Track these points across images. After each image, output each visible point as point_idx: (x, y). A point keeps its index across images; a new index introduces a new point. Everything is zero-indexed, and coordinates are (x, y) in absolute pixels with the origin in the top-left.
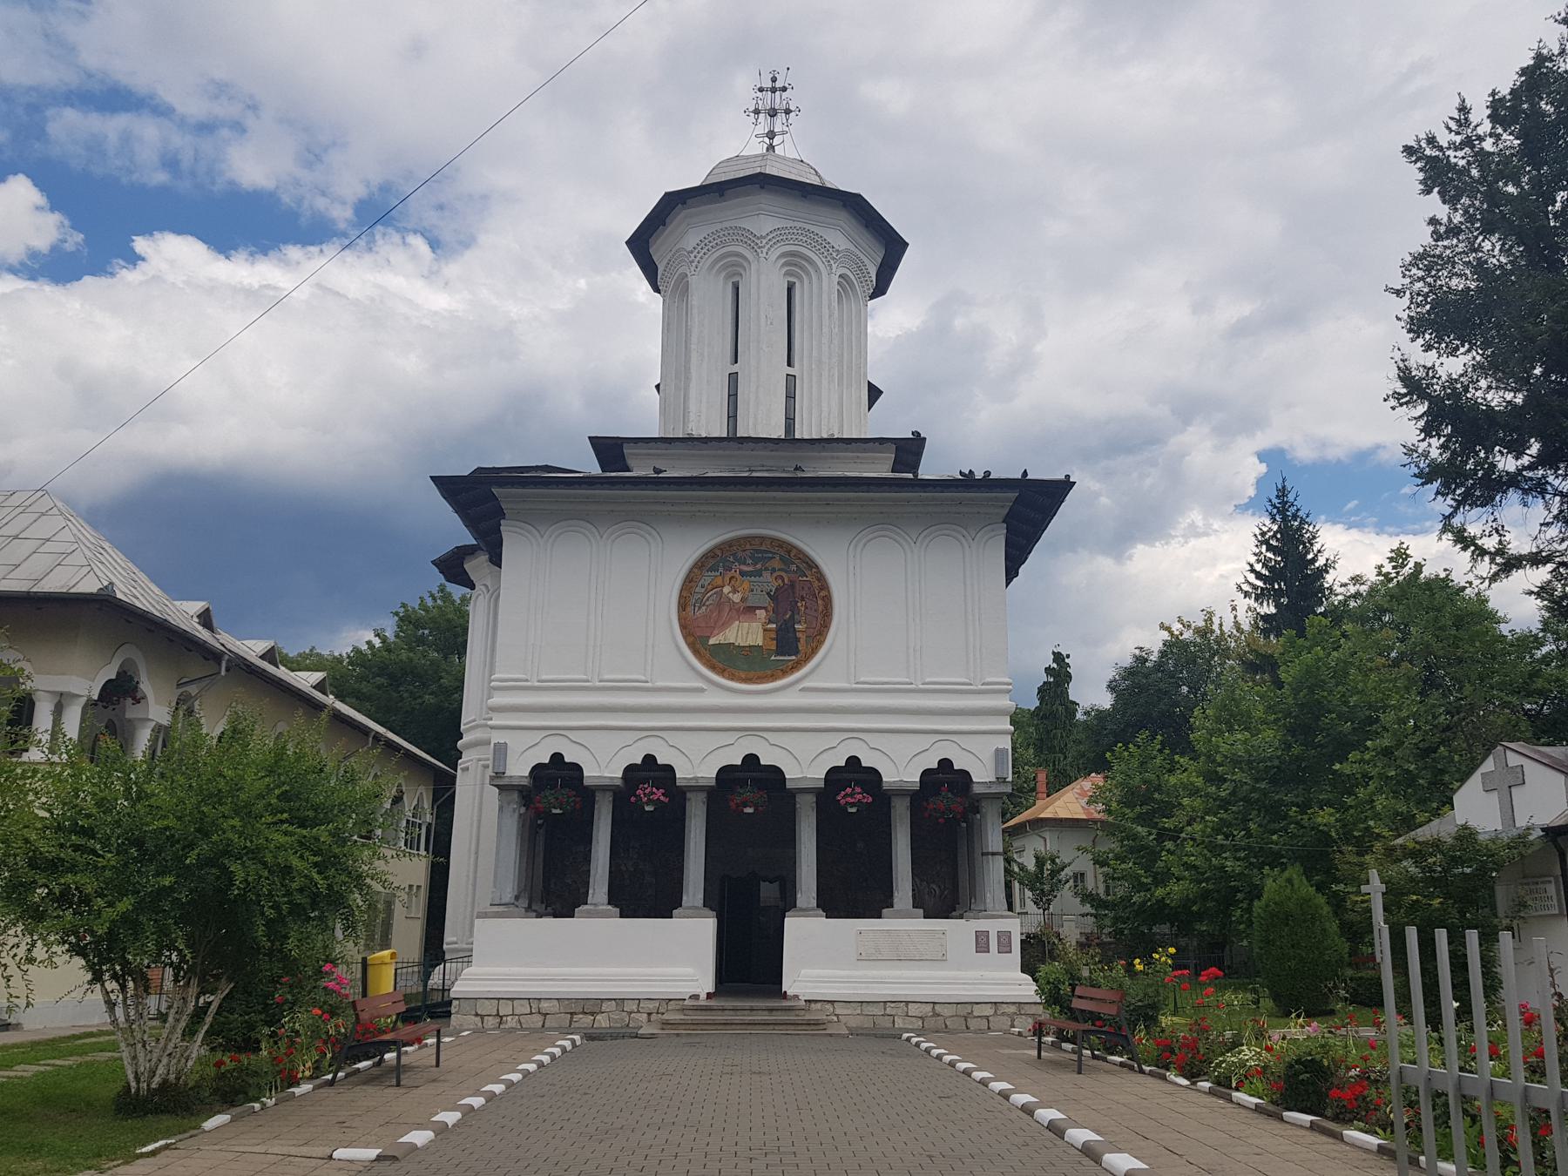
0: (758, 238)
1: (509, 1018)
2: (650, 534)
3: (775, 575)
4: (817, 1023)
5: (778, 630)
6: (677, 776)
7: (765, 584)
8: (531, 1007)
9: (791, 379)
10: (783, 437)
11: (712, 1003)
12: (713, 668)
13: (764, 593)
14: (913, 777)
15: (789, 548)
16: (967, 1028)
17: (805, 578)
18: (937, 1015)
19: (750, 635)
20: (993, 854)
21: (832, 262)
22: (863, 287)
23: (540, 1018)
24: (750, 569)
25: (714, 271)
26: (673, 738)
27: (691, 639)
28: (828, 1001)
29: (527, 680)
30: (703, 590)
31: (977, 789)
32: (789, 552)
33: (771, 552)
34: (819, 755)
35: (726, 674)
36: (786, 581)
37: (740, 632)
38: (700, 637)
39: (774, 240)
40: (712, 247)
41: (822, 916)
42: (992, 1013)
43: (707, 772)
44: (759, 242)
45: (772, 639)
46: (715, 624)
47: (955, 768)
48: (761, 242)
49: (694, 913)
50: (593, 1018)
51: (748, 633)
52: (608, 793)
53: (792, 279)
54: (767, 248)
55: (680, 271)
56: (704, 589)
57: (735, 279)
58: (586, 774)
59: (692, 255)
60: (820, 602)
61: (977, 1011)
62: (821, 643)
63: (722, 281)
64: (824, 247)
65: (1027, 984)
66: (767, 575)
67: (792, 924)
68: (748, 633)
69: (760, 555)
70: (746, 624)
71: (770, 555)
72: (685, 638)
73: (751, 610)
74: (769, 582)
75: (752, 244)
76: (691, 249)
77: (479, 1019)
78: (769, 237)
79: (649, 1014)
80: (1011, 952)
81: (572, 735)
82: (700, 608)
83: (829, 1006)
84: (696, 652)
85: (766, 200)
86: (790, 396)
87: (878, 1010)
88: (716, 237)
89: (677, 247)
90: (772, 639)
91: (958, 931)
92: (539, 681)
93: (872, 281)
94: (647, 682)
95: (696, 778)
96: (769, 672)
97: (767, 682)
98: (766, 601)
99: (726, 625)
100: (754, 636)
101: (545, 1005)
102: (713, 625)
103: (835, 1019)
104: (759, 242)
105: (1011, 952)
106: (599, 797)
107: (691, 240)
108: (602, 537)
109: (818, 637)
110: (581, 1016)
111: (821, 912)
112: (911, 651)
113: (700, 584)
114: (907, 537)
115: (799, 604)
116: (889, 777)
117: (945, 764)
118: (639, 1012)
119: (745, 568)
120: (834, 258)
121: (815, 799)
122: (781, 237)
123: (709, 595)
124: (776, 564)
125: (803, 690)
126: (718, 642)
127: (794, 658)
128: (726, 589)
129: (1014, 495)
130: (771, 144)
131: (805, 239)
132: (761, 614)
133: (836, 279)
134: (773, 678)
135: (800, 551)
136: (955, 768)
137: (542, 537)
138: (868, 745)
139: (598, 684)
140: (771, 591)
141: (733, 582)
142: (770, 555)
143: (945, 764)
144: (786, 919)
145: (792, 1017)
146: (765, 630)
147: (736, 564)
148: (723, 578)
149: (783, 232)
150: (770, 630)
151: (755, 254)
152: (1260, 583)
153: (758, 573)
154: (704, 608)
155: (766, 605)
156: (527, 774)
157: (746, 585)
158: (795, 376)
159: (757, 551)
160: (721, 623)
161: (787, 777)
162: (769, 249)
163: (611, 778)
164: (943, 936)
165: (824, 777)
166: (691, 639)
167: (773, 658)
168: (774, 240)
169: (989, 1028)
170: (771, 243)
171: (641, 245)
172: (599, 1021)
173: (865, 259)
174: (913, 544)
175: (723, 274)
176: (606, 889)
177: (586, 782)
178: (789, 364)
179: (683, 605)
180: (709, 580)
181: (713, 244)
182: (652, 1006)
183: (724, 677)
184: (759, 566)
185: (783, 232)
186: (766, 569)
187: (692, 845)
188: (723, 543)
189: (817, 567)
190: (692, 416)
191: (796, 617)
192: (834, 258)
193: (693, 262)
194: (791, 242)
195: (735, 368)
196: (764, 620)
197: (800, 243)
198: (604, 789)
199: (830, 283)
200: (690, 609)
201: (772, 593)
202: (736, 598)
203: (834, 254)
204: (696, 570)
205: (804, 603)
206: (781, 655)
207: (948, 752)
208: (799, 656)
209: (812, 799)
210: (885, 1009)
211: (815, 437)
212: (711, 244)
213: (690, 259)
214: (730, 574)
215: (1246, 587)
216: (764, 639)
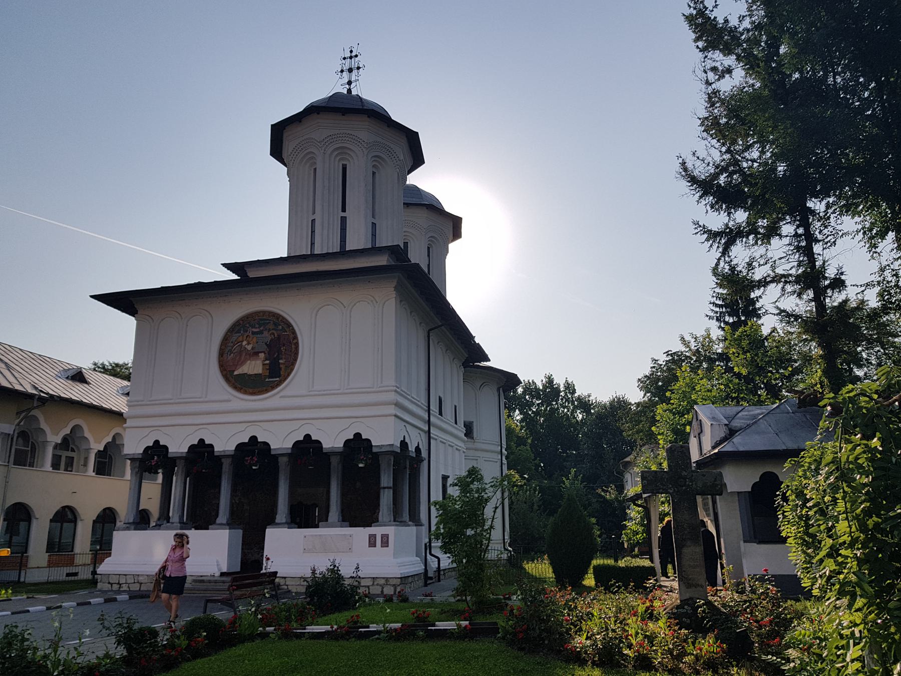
1: (124, 585)
3: (271, 332)
5: (270, 364)
6: (215, 450)
11: (224, 579)
14: (339, 444)
20: (384, 488)
21: (364, 149)
23: (138, 585)
25: (305, 161)
27: (225, 372)
28: (283, 577)
29: (142, 401)
31: (375, 450)
32: (278, 319)
33: (267, 320)
34: (289, 434)
35: (242, 390)
38: (230, 371)
39: (329, 142)
41: (285, 528)
42: (371, 583)
43: (231, 447)
44: (319, 144)
45: (267, 369)
47: (363, 438)
49: (221, 526)
52: (182, 461)
54: (323, 148)
58: (170, 451)
60: (293, 346)
62: (292, 370)
66: (266, 334)
67: (270, 532)
68: (254, 367)
70: (254, 362)
71: (268, 321)
72: (222, 372)
73: (256, 354)
74: (267, 336)
77: (110, 585)
80: (388, 546)
82: (230, 355)
90: (267, 369)
91: (361, 534)
95: (224, 451)
96: (265, 388)
97: (264, 394)
99: (243, 363)
101: (141, 578)
103: (286, 587)
104: (319, 144)
105: (388, 546)
106: (178, 461)
116: (327, 445)
117: (358, 435)
119: (255, 330)
121: (287, 460)
124: (271, 326)
125: (281, 397)
127: (278, 379)
128: (244, 343)
131: (347, 139)
132: (262, 355)
134: (267, 391)
135: (283, 318)
136: (363, 438)
142: (268, 321)
143: (358, 435)
144: (267, 530)
146: (263, 365)
152: (717, 309)
153: (261, 332)
156: (142, 452)
157: (255, 340)
159: (261, 320)
161: (272, 447)
163: (182, 453)
164: (349, 537)
166: (225, 372)
167: (267, 380)
168: (329, 142)
170: (327, 144)
173: (392, 146)
175: (308, 164)
177: (170, 455)
179: (221, 353)
180: (235, 338)
181: (300, 149)
183: (241, 392)
184: (262, 328)
186: (266, 330)
189: (292, 326)
198: (180, 458)
200: (225, 355)
202: (249, 347)
203: (365, 145)
209: (285, 459)
211: (335, 251)
215: (712, 314)
216: (263, 369)
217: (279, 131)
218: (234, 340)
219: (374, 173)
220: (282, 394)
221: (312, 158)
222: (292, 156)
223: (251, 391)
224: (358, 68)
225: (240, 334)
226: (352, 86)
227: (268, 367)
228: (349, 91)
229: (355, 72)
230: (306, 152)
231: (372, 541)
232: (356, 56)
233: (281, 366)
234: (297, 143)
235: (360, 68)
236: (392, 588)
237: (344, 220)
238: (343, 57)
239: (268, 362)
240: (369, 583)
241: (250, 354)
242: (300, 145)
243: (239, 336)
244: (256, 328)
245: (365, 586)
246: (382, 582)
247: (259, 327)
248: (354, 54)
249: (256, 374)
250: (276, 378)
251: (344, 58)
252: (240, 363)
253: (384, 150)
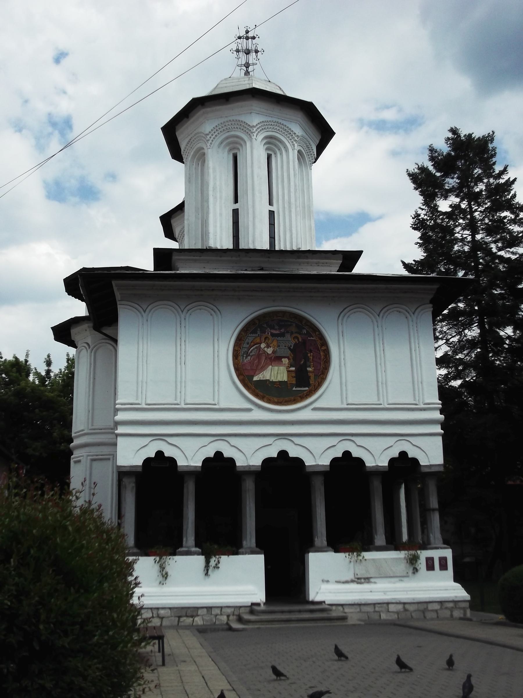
0: (251, 127)
2: (215, 312)
4: (344, 619)
5: (296, 372)
7: (287, 342)
8: (153, 614)
10: (269, 249)
12: (256, 395)
13: (287, 348)
16: (425, 617)
17: (312, 338)
18: (406, 610)
19: (279, 375)
21: (294, 143)
22: (309, 158)
24: (277, 332)
26: (233, 441)
30: (248, 346)
36: (300, 340)
37: (273, 373)
39: (260, 129)
40: (221, 132)
45: (293, 377)
46: (257, 368)
48: (253, 130)
50: (192, 619)
53: (270, 152)
54: (256, 132)
55: (199, 145)
56: (248, 346)
57: (235, 151)
59: (208, 137)
60: (322, 353)
61: (431, 607)
63: (227, 152)
64: (290, 133)
65: (458, 589)
66: (288, 337)
69: (283, 323)
70: (276, 368)
71: (289, 323)
72: (238, 376)
74: (290, 341)
75: (247, 131)
76: (207, 132)
78: (257, 127)
79: (228, 616)
81: (170, 440)
82: (246, 357)
83: (340, 608)
85: (256, 105)
87: (370, 609)
88: (223, 125)
89: (195, 132)
90: (293, 377)
92: (146, 404)
93: (314, 155)
94: (216, 405)
96: (293, 398)
98: (288, 353)
99: (263, 368)
100: (282, 375)
101: (162, 612)
102: (255, 368)
104: (251, 129)
107: (208, 127)
108: (182, 312)
109: (322, 376)
110: (185, 618)
111: (331, 549)
112: (380, 384)
113: (246, 342)
114: (373, 312)
115: (309, 355)
118: (221, 614)
120: (295, 141)
122: (264, 127)
123: (252, 348)
126: (259, 379)
127: (307, 389)
128: (263, 346)
129: (436, 287)
130: (247, 71)
131: (278, 128)
132: (285, 361)
133: (296, 152)
134: (295, 401)
137: (145, 311)
138: (356, 444)
139: (183, 406)
140: (291, 346)
141: (267, 341)
142: (289, 323)
143: (403, 454)
145: (324, 615)
146: (289, 371)
147: (268, 329)
148: (261, 338)
149: (265, 124)
150: (291, 371)
151: (249, 136)
153: (282, 335)
154: (249, 357)
155: (288, 355)
157: (275, 343)
158: (274, 212)
160: (260, 368)
162: (257, 134)
163: (196, 467)
165: (329, 464)
166: (242, 377)
167: (294, 389)
168: (260, 129)
169: (438, 617)
172: (197, 621)
173: (311, 142)
174: (378, 317)
175: (228, 148)
176: (193, 538)
178: (271, 203)
179: (236, 356)
181: (222, 130)
182: (229, 611)
183: (264, 401)
184: (282, 330)
185: (265, 124)
186: (288, 332)
187: (248, 508)
190: (211, 236)
191: (308, 363)
192: (295, 141)
193: (208, 140)
194: (270, 130)
195: (236, 206)
196: (287, 365)
197: (276, 131)
199: (293, 155)
200: (240, 358)
201: (292, 348)
202: (270, 351)
203: (296, 138)
204: (243, 333)
205: (312, 354)
206: (301, 387)
207: (405, 447)
208: (310, 388)
210: (375, 608)
212: (220, 130)
213: (207, 139)
214: (264, 336)
216: (288, 377)
218: (250, 341)
220: (316, 405)
221: (236, 143)
222: (210, 135)
223: (276, 400)
224: (257, 52)
225: (257, 335)
226: (250, 69)
227: (294, 375)
230: (227, 134)
231: (430, 563)
232: (254, 38)
233: (310, 374)
234: (217, 124)
235: (259, 51)
236: (462, 611)
238: (238, 35)
239: (293, 369)
240: (437, 607)
241: (270, 359)
242: (223, 125)
243: (256, 337)
244: (276, 330)
245: (432, 611)
246: (451, 605)
247: (280, 329)
248: (250, 35)
249: (280, 382)
250: (305, 387)
251: (240, 38)
252: (260, 367)
253: (305, 145)
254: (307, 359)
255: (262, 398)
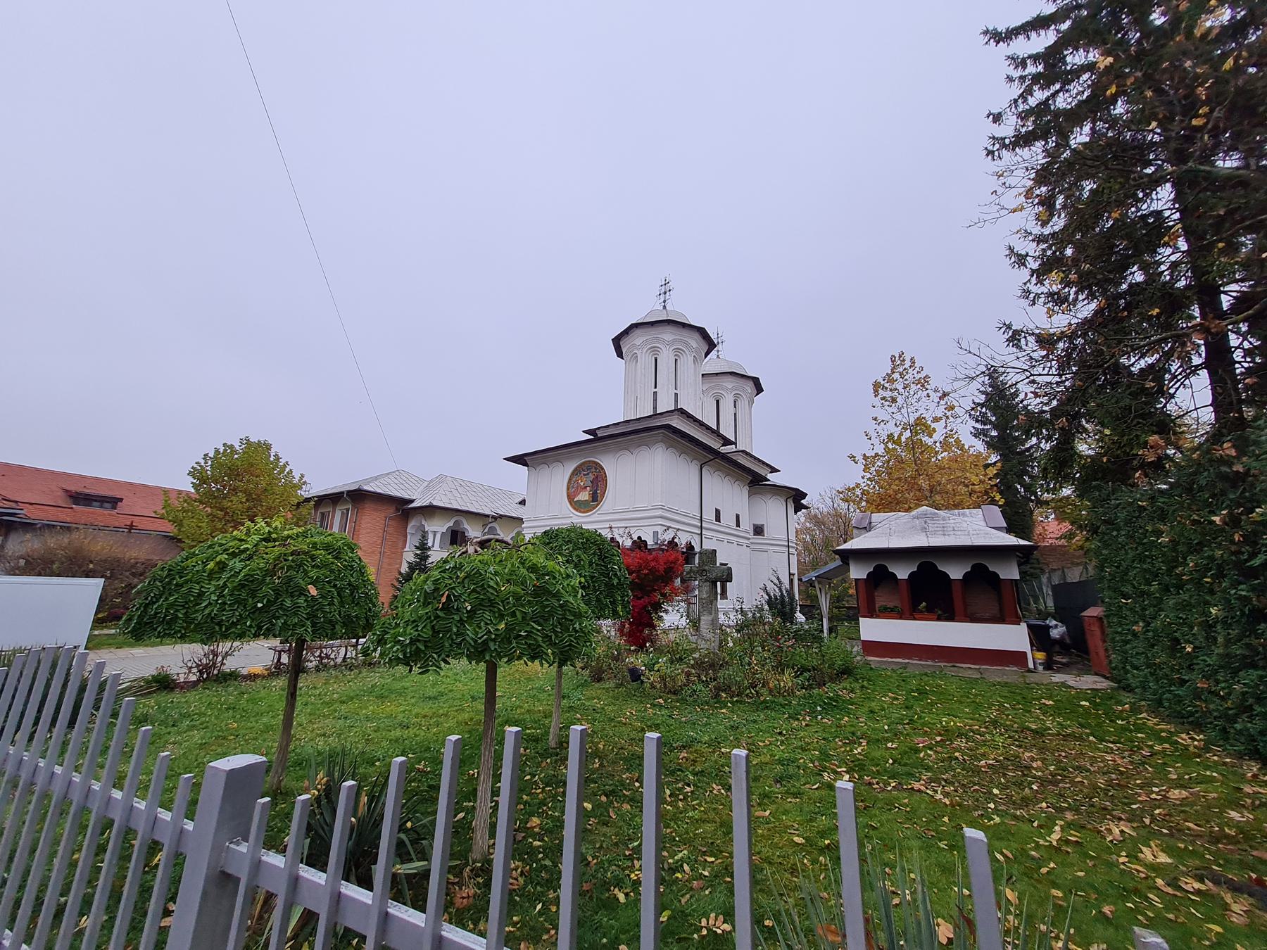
9: (655, 393)
12: (575, 509)
15: (597, 463)
51: (584, 496)
64: (663, 341)
74: (591, 477)
84: (571, 504)
85: (638, 332)
86: (655, 400)
124: (593, 470)
134: (591, 510)
153: (588, 474)
171: (620, 354)
179: (568, 489)
188: (578, 467)
202: (582, 484)
217: (617, 342)
219: (676, 360)
228: (664, 307)
229: (668, 293)
237: (655, 393)
254: (597, 486)
255: (577, 510)
